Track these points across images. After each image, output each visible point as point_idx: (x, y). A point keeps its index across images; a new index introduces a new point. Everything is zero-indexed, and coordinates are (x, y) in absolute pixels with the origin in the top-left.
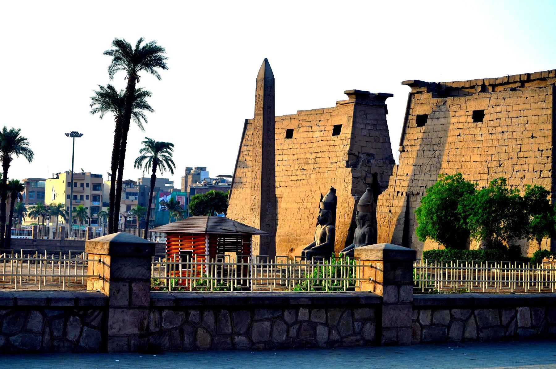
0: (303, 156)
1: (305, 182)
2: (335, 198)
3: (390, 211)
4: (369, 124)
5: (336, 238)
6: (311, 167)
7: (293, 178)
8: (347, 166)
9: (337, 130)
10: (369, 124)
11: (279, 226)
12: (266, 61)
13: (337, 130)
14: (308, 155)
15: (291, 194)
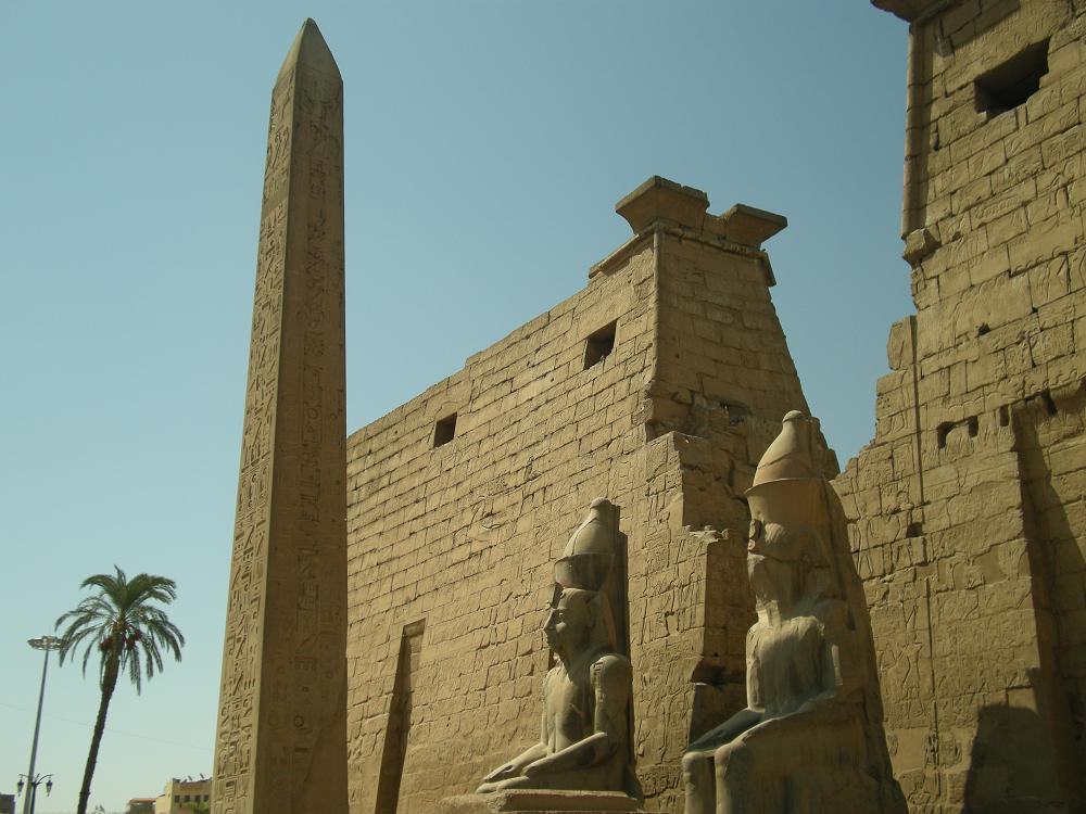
0: (487, 474)
1: (497, 554)
2: (619, 543)
3: (914, 530)
4: (719, 307)
5: (641, 725)
6: (517, 496)
7: (458, 555)
8: (654, 429)
9: (600, 345)
10: (719, 307)
11: (413, 729)
12: (311, 28)
13: (600, 345)
14: (504, 466)
15: (452, 609)
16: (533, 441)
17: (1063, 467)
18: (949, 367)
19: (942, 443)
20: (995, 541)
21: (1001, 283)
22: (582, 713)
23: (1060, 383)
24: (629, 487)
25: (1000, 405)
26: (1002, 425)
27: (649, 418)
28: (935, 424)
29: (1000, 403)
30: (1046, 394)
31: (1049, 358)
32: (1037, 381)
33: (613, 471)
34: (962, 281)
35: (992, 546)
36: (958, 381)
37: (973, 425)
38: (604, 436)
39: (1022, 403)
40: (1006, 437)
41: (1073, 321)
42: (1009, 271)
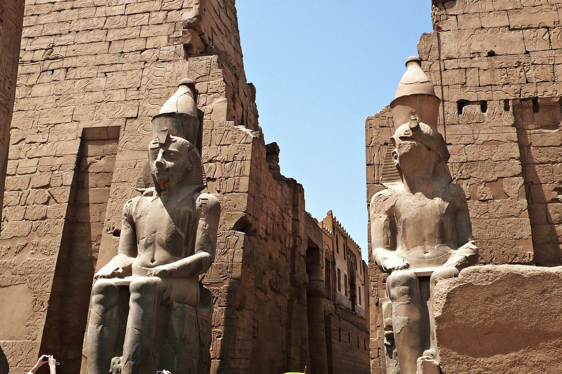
16: (54, 33)
17: (539, 143)
18: (466, 68)
19: (460, 112)
20: (502, 175)
21: (503, 31)
22: (183, 235)
23: (545, 96)
24: (165, 84)
25: (504, 98)
26: (505, 110)
27: (188, 41)
28: (456, 98)
29: (505, 97)
30: (535, 100)
31: (538, 80)
32: (530, 91)
33: (146, 71)
34: (475, 22)
35: (498, 178)
36: (472, 78)
37: (484, 105)
38: (140, 44)
39: (518, 101)
40: (508, 117)
41: (553, 65)
42: (509, 26)
